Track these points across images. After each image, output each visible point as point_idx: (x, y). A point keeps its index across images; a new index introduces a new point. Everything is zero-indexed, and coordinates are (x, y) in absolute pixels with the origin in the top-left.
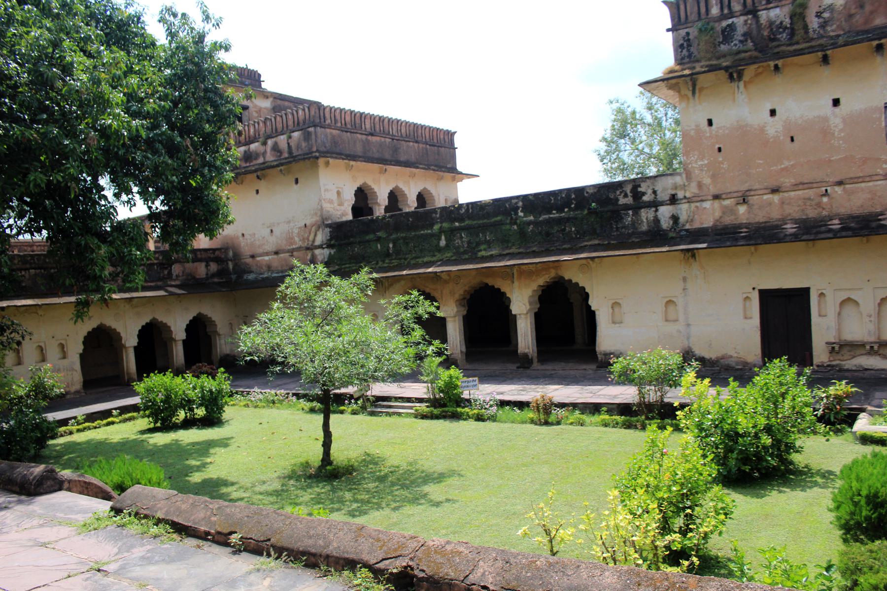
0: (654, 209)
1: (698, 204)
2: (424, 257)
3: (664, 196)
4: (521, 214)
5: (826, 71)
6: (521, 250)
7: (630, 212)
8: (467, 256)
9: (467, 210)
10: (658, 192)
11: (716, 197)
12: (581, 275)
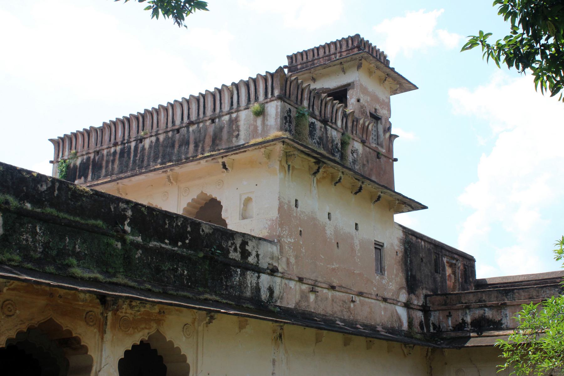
0: (256, 275)
1: (287, 281)
3: (264, 264)
4: (128, 228)
5: (353, 199)
7: (239, 270)
9: (51, 189)
10: (260, 257)
11: (301, 280)
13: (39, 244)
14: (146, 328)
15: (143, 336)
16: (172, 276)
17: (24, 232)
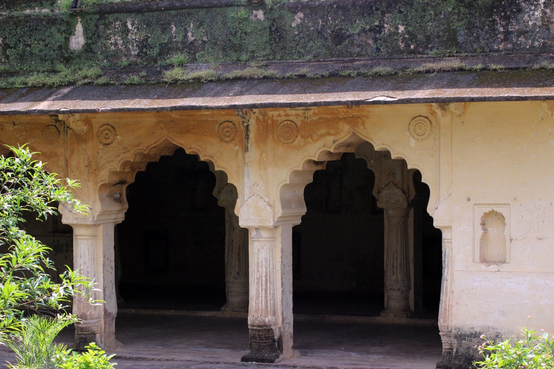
2: (29, 73)
6: (270, 72)
8: (136, 79)
12: (413, 142)
13: (133, 46)
14: (329, 134)
15: (324, 146)
16: (371, 42)
17: (110, 34)
